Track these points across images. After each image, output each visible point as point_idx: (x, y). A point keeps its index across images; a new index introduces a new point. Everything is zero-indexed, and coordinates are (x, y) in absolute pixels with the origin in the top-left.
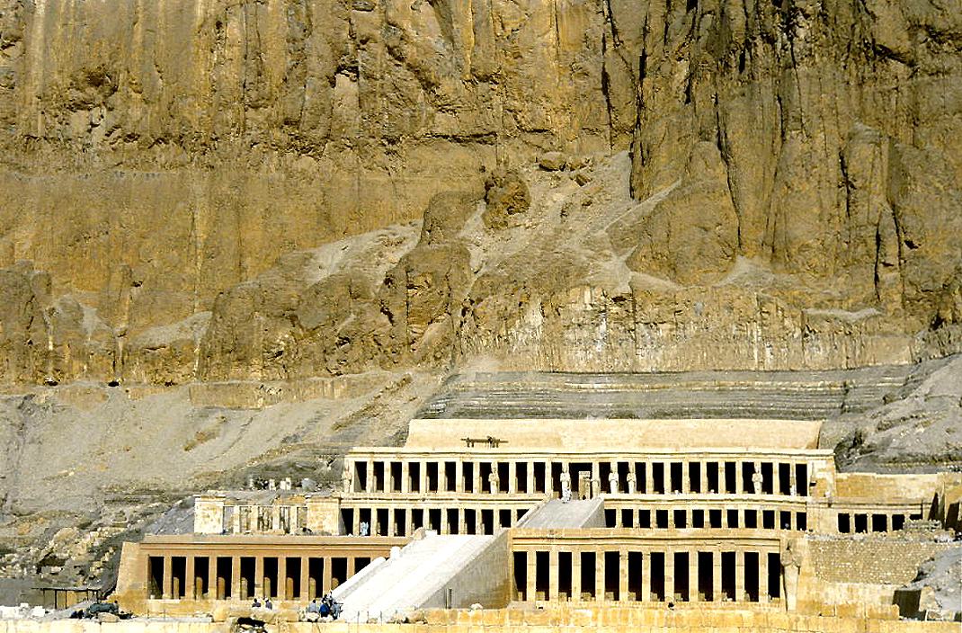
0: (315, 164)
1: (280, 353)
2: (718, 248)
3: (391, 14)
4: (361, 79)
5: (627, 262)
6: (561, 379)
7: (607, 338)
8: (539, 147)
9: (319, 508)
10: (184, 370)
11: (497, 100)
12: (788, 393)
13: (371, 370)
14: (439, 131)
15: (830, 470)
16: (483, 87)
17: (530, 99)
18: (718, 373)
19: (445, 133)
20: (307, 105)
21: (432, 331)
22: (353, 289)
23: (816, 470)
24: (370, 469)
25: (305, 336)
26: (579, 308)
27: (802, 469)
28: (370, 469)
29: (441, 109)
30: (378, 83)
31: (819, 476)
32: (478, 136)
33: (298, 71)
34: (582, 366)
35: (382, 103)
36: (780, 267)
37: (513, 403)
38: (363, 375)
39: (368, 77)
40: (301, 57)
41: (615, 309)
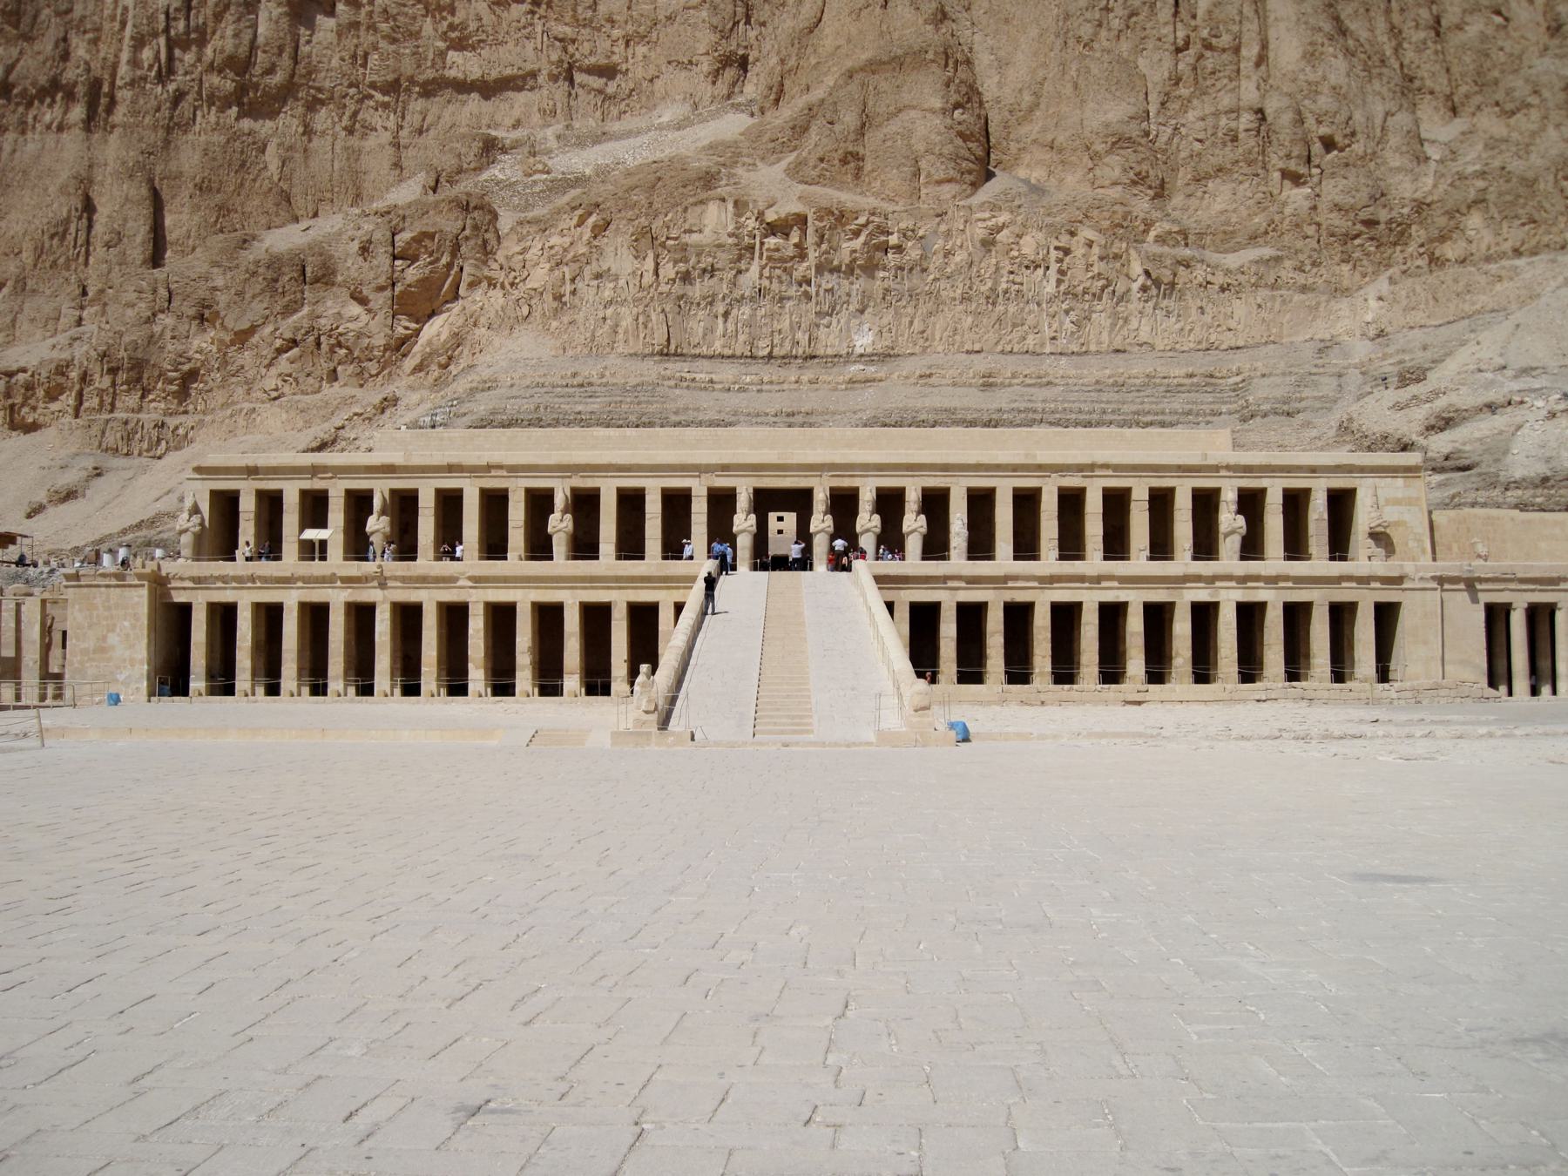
0: (269, 124)
1: (192, 375)
2: (959, 141)
5: (788, 171)
6: (675, 367)
8: (600, 92)
9: (98, 601)
10: (54, 406)
11: (539, 29)
12: (1119, 386)
13: (332, 391)
14: (452, 73)
15: (1410, 502)
17: (587, 24)
18: (973, 356)
19: (460, 76)
20: (261, 40)
21: (436, 330)
22: (309, 270)
23: (1382, 502)
24: (247, 505)
25: (233, 343)
26: (705, 238)
27: (1341, 503)
28: (247, 505)
29: (460, 45)
30: (363, 11)
31: (1391, 514)
34: (718, 346)
35: (367, 39)
36: (1070, 179)
37: (579, 408)
38: (318, 396)
41: (772, 241)
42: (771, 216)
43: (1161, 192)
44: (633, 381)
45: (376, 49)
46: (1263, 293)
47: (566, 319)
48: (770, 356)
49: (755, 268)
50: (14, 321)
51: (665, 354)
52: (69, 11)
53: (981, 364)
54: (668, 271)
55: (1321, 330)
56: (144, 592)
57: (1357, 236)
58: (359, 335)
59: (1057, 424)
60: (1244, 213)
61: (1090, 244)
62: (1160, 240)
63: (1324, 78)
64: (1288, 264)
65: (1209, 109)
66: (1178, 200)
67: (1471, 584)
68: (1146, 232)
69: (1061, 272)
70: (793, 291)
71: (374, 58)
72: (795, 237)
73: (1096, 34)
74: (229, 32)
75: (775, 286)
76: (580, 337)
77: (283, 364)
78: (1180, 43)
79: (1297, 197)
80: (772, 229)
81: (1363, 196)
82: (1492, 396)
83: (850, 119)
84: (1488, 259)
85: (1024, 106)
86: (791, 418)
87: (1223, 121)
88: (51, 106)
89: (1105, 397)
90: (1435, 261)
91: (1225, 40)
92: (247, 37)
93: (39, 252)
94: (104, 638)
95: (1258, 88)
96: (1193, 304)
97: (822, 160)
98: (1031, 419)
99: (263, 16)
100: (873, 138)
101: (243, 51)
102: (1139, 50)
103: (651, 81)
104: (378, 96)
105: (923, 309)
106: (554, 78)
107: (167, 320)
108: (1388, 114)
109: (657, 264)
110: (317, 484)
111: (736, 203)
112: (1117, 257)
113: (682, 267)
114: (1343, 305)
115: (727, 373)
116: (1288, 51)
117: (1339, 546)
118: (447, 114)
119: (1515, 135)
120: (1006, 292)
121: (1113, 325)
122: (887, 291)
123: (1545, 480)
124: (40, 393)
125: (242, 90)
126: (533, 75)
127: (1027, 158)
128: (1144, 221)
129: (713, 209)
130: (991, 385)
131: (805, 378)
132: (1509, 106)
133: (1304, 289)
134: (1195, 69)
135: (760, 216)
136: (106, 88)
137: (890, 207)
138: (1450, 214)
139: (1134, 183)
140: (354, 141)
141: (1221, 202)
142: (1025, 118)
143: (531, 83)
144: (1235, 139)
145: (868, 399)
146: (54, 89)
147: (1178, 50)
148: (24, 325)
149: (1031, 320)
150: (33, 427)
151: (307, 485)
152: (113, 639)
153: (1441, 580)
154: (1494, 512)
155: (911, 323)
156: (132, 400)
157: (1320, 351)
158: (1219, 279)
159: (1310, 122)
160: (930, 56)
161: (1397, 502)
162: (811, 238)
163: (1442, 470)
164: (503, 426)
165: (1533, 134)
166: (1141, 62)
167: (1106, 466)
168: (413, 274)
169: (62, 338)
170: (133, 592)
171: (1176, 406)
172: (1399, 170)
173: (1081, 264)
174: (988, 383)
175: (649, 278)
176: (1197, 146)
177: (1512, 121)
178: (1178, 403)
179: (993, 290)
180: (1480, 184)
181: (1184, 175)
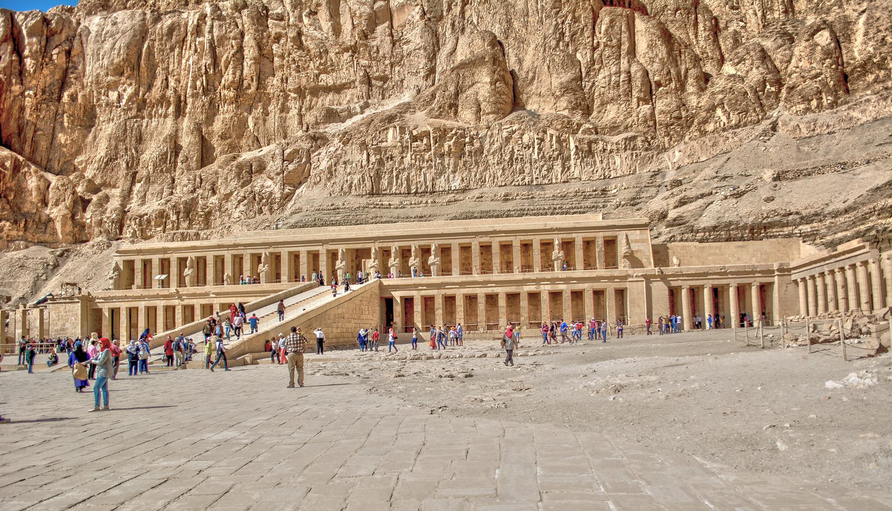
1: (209, 213)
2: (498, 95)
3: (291, 20)
4: (276, 59)
7: (411, 166)
8: (381, 87)
13: (259, 218)
14: (322, 83)
15: (643, 241)
16: (346, 55)
17: (375, 59)
20: (244, 75)
24: (138, 266)
25: (224, 199)
27: (610, 243)
28: (138, 266)
29: (325, 71)
31: (634, 247)
32: (345, 84)
33: (238, 56)
35: (287, 72)
39: (279, 57)
40: (241, 49)
42: (415, 133)
43: (587, 111)
44: (356, 206)
45: (290, 74)
46: (629, 152)
47: (332, 182)
48: (416, 193)
49: (409, 155)
50: (145, 195)
51: (372, 194)
52: (168, 67)
53: (503, 191)
54: (373, 159)
55: (653, 167)
56: (79, 304)
57: (672, 125)
58: (271, 193)
59: (534, 215)
60: (622, 118)
61: (552, 136)
62: (584, 132)
63: (657, 55)
64: (639, 139)
65: (607, 73)
66: (595, 114)
67: (663, 277)
68: (578, 130)
69: (540, 149)
70: (425, 165)
71: (290, 79)
72: (425, 141)
73: (557, 45)
74: (231, 72)
75: (417, 163)
76: (338, 189)
77: (242, 207)
78: (595, 45)
79: (645, 109)
80: (415, 139)
81: (674, 105)
82: (706, 190)
83: (452, 89)
84: (724, 130)
85: (529, 78)
86: (421, 218)
87: (613, 78)
88: (162, 107)
89: (555, 202)
90: (704, 133)
91: (615, 41)
92: (238, 74)
93: (155, 167)
94: (64, 325)
95: (628, 62)
96: (598, 160)
97: (440, 108)
98: (522, 213)
99: (245, 64)
100: (462, 97)
101: (237, 78)
102: (576, 50)
103: (402, 81)
104: (293, 95)
105: (481, 168)
106: (361, 83)
107: (200, 191)
108: (687, 70)
109: (368, 155)
110: (166, 256)
111: (400, 128)
112: (565, 141)
113: (378, 157)
114: (665, 156)
115: (396, 201)
116: (642, 45)
117: (611, 261)
118: (320, 100)
119: (739, 73)
120: (517, 159)
121: (562, 171)
122: (466, 162)
123: (715, 228)
124: (153, 223)
125: (237, 97)
126: (354, 82)
127: (530, 101)
128: (577, 124)
129: (391, 131)
130: (507, 200)
131: (429, 201)
132: (736, 60)
133: (647, 150)
134: (601, 56)
135: (411, 133)
136: (182, 98)
137: (466, 126)
138: (708, 111)
139: (573, 109)
140: (284, 114)
141: (612, 113)
142: (530, 84)
143: (352, 86)
144: (618, 86)
145: (454, 209)
146: (163, 100)
147: (594, 49)
148: (149, 196)
149: (527, 171)
150: (151, 237)
151: (161, 256)
152: (68, 325)
153: (645, 276)
154: (686, 244)
155: (476, 175)
156: (185, 225)
157: (652, 176)
158: (609, 148)
159: (651, 75)
160: (487, 59)
161: (637, 241)
162: (432, 142)
163: (672, 226)
164: (300, 227)
165: (748, 72)
166: (579, 56)
167: (500, 232)
168: (291, 167)
169: (163, 201)
170: (75, 305)
171: (588, 203)
172: (692, 93)
173: (548, 144)
174: (506, 198)
175: (364, 163)
176: (603, 90)
177: (738, 67)
178: (588, 203)
179: (511, 159)
180: (721, 96)
181: (597, 103)
